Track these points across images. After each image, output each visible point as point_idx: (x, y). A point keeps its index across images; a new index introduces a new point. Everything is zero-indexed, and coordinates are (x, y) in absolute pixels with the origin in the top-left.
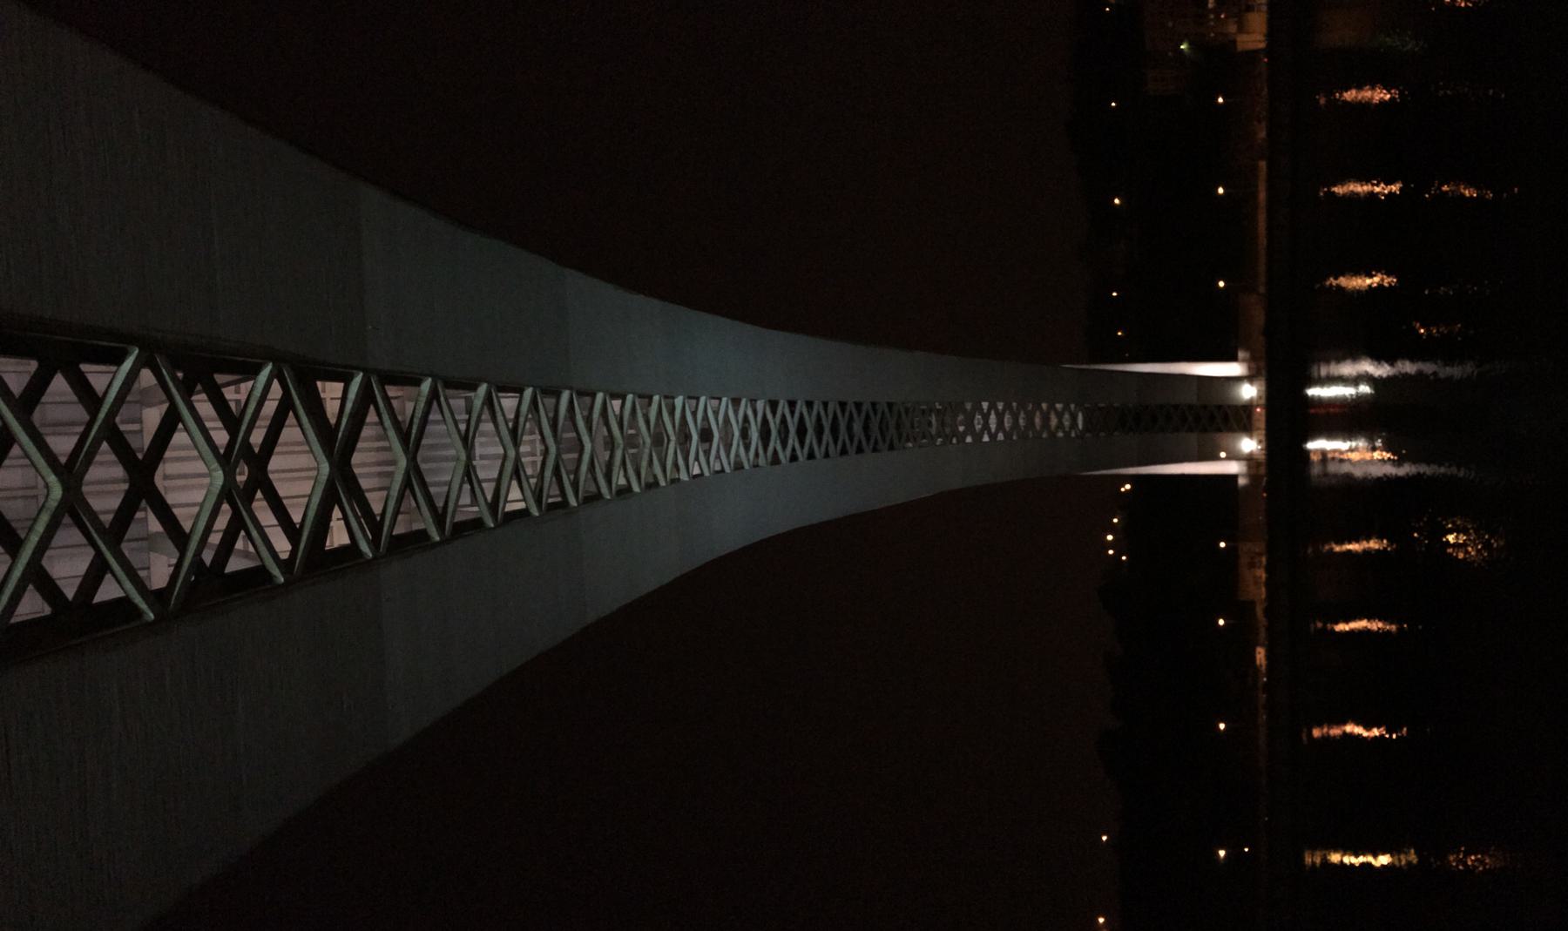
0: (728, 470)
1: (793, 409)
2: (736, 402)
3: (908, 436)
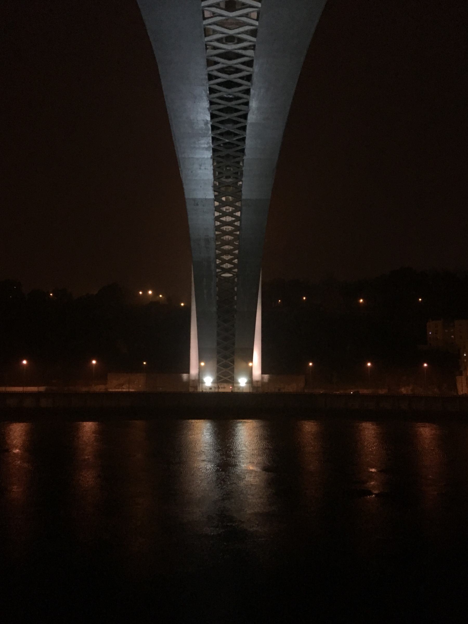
0: (205, 22)
1: (245, 79)
2: (253, 33)
3: (222, 162)
